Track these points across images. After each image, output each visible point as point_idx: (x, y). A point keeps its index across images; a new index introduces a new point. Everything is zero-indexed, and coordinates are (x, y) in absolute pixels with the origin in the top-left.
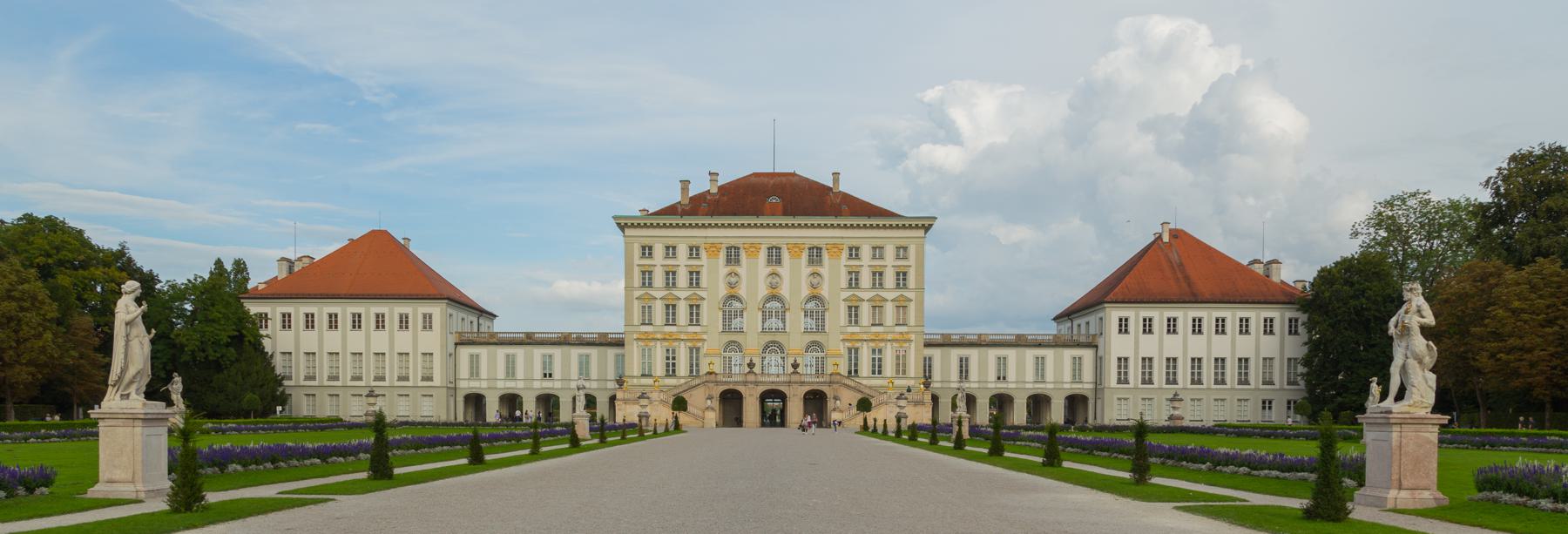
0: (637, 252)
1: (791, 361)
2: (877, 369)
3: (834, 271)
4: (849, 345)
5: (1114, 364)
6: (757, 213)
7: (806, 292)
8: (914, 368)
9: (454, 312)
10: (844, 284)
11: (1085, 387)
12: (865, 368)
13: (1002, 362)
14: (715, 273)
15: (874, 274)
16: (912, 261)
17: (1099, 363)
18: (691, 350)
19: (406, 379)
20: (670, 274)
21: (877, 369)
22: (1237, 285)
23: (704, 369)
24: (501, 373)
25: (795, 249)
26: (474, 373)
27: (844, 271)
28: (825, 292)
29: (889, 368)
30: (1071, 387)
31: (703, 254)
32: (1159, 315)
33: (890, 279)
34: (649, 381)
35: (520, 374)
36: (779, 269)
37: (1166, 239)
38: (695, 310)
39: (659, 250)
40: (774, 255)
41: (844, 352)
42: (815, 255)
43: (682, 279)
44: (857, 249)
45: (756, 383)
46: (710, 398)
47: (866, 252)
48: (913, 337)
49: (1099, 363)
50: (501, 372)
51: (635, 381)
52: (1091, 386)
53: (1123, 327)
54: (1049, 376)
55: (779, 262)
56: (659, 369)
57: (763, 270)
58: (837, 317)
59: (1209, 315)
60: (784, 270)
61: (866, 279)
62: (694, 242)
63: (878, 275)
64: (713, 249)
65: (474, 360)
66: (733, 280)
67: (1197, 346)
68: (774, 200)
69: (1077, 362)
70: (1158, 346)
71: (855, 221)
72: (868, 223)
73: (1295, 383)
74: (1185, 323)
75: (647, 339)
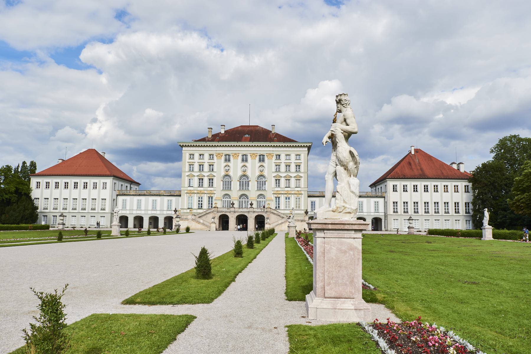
0: (188, 156)
1: (250, 202)
3: (270, 164)
4: (276, 196)
5: (392, 204)
7: (258, 173)
9: (117, 182)
10: (274, 170)
12: (282, 206)
14: (220, 165)
15: (296, 166)
16: (302, 160)
18: (209, 197)
19: (94, 209)
20: (201, 166)
22: (445, 172)
25: (253, 155)
26: (124, 207)
27: (274, 165)
28: (265, 173)
31: (215, 157)
32: (410, 184)
33: (293, 168)
34: (188, 211)
35: (143, 208)
36: (246, 164)
37: (413, 153)
38: (211, 180)
39: (197, 156)
40: (245, 159)
41: (274, 199)
42: (262, 159)
43: (206, 168)
44: (279, 156)
45: (235, 212)
46: (214, 218)
47: (283, 157)
48: (303, 192)
49: (386, 203)
51: (185, 211)
52: (383, 214)
53: (395, 189)
55: (247, 161)
56: (195, 206)
57: (240, 164)
58: (271, 184)
59: (431, 184)
60: (249, 164)
61: (283, 168)
62: (211, 153)
64: (219, 155)
65: (124, 202)
66: (227, 168)
67: (427, 197)
69: (377, 203)
70: (410, 197)
71: (278, 144)
72: (283, 145)
73: (469, 213)
74: (421, 188)
75: (190, 193)
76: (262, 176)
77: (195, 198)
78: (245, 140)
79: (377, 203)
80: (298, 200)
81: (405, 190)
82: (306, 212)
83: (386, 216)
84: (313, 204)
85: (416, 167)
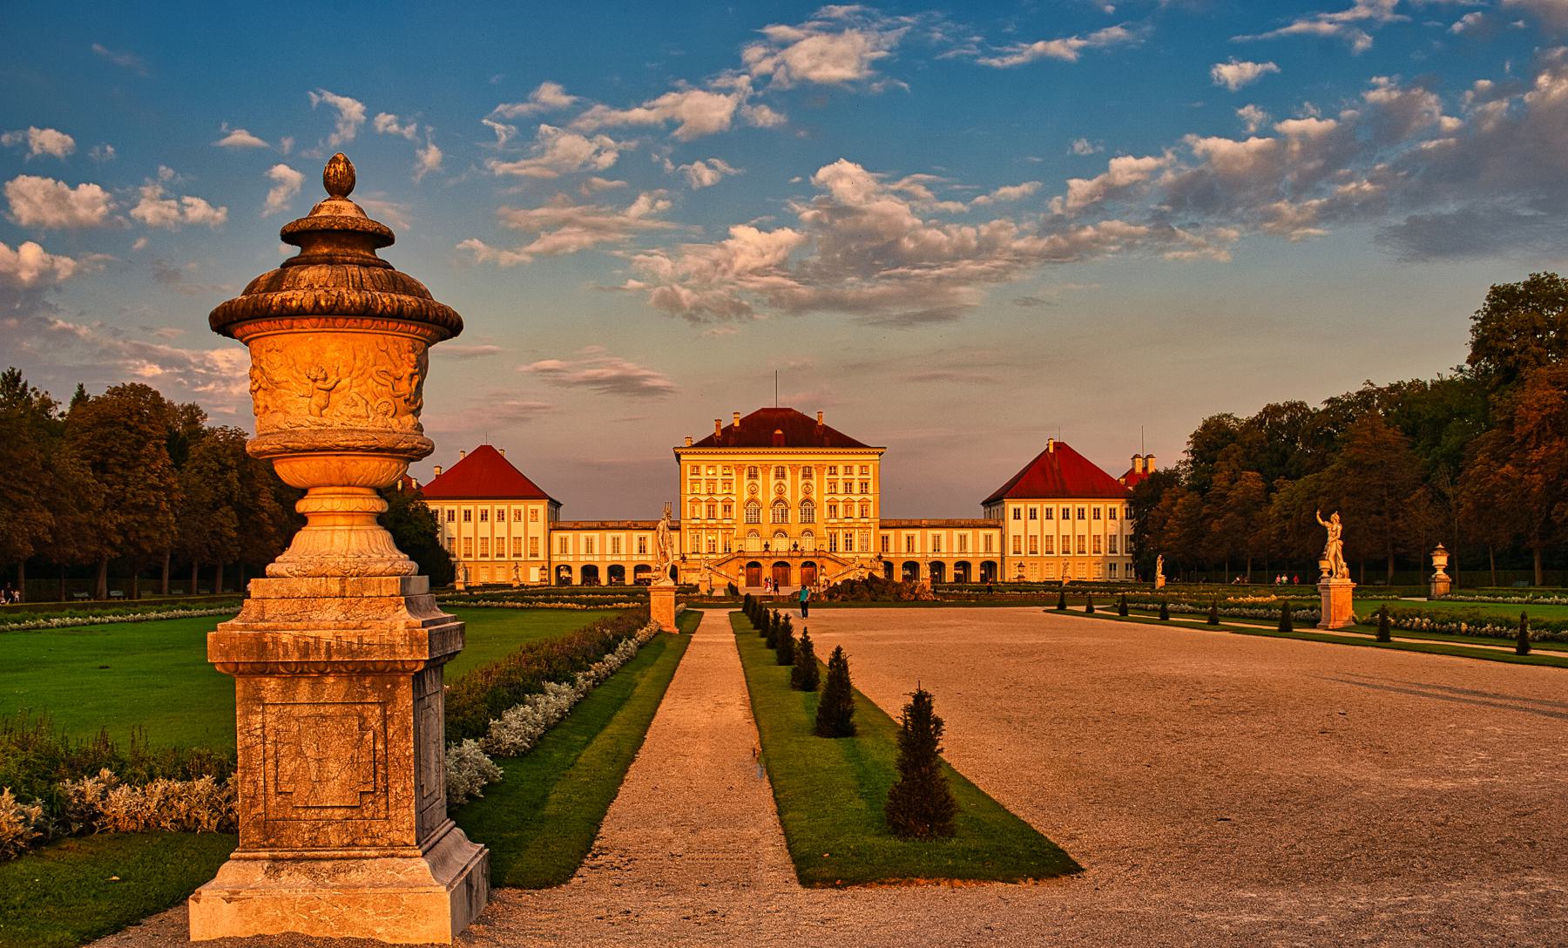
2: (849, 545)
6: (770, 446)
7: (801, 497)
8: (874, 546)
11: (995, 555)
12: (841, 546)
13: (937, 539)
21: (849, 545)
23: (734, 550)
24: (583, 550)
26: (564, 550)
28: (814, 496)
29: (856, 548)
30: (984, 556)
33: (856, 488)
35: (596, 550)
38: (727, 508)
40: (780, 474)
42: (807, 475)
47: (841, 470)
49: (1003, 537)
53: (1017, 515)
54: (970, 548)
55: (783, 476)
57: (773, 482)
60: (787, 482)
63: (848, 487)
64: (739, 468)
65: (564, 542)
68: (779, 432)
69: (988, 538)
75: (696, 528)
76: (807, 500)
78: (779, 446)
79: (988, 538)
81: (1033, 516)
82: (880, 557)
83: (1002, 558)
84: (885, 539)
85: (1059, 474)
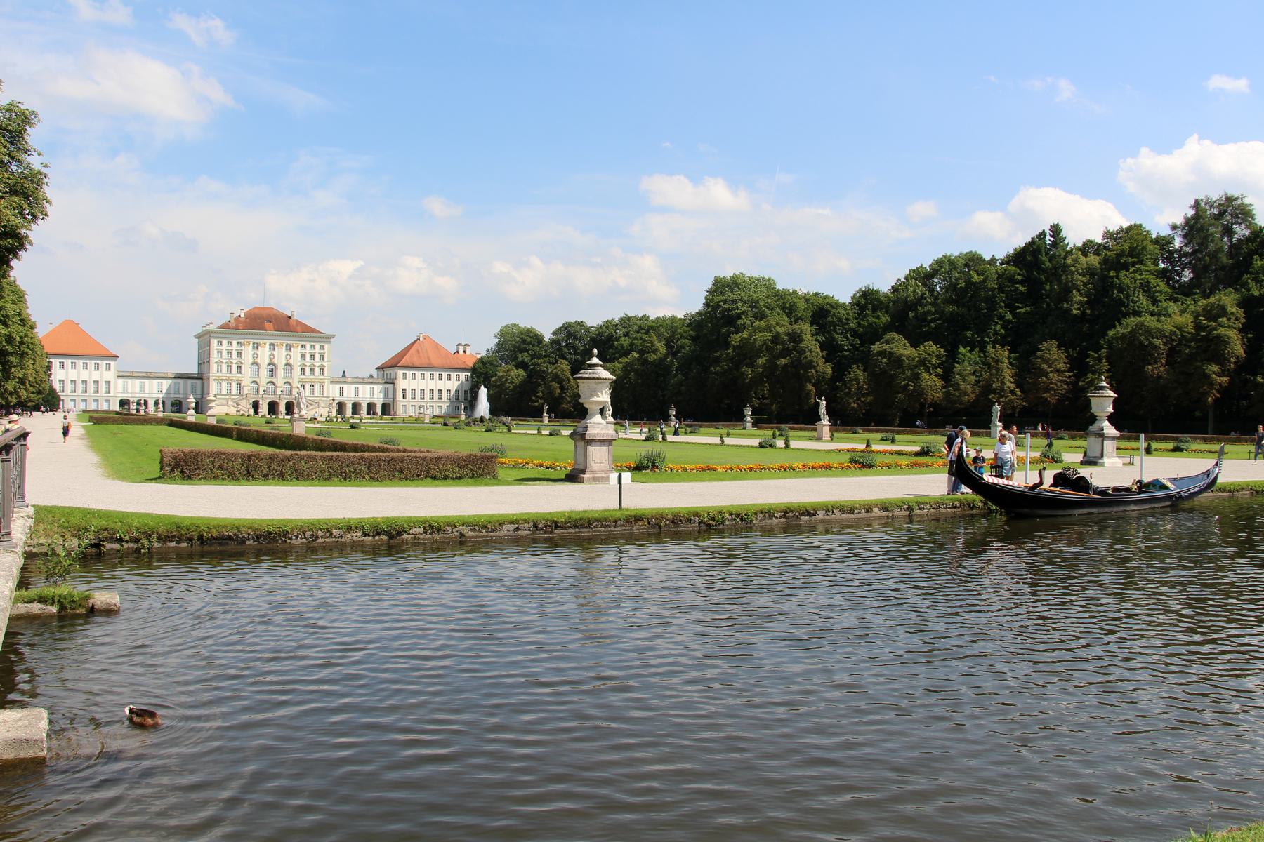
3: (296, 353)
7: (284, 362)
11: (389, 400)
14: (248, 352)
17: (395, 390)
20: (230, 353)
21: (313, 392)
29: (317, 393)
42: (289, 347)
43: (235, 354)
50: (138, 390)
56: (224, 392)
58: (297, 370)
60: (275, 353)
61: (308, 357)
67: (432, 385)
77: (224, 384)
80: (322, 387)
